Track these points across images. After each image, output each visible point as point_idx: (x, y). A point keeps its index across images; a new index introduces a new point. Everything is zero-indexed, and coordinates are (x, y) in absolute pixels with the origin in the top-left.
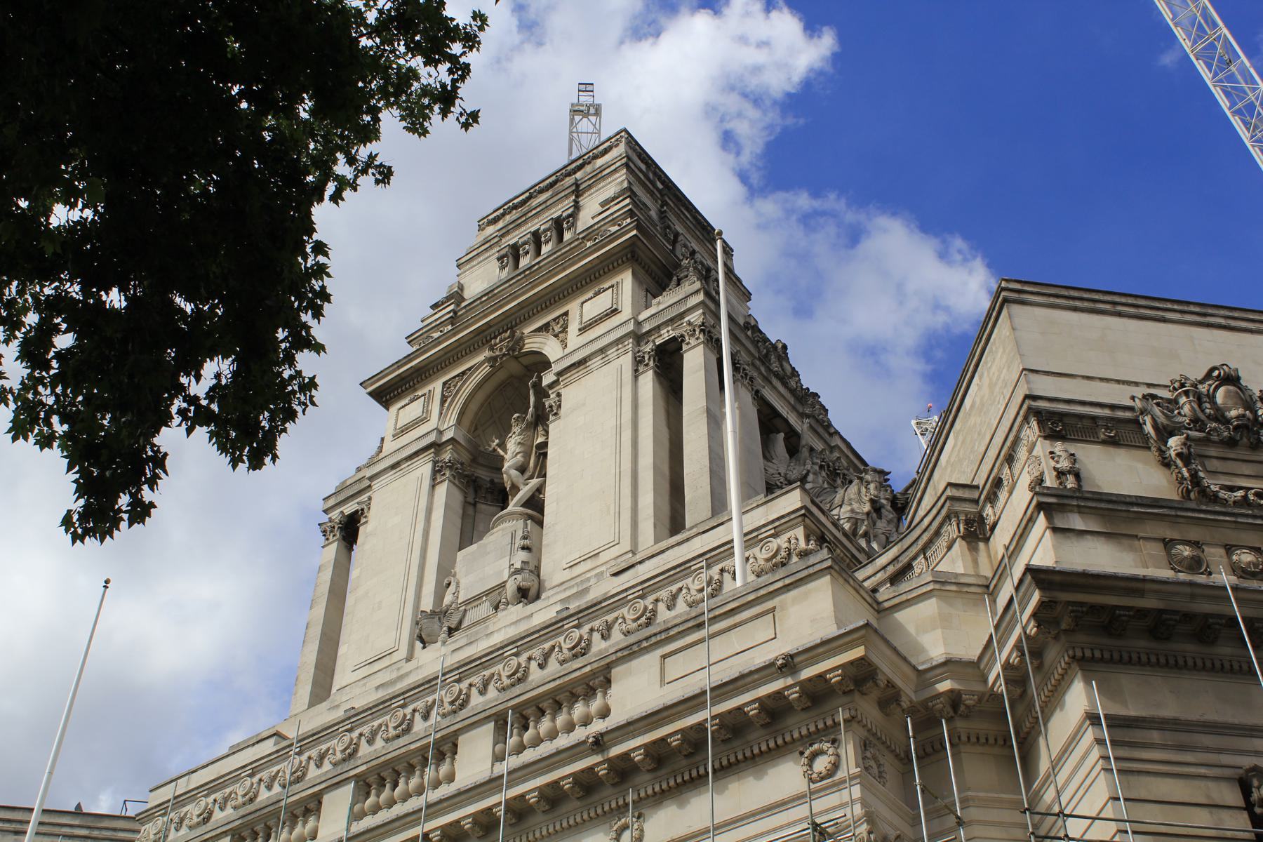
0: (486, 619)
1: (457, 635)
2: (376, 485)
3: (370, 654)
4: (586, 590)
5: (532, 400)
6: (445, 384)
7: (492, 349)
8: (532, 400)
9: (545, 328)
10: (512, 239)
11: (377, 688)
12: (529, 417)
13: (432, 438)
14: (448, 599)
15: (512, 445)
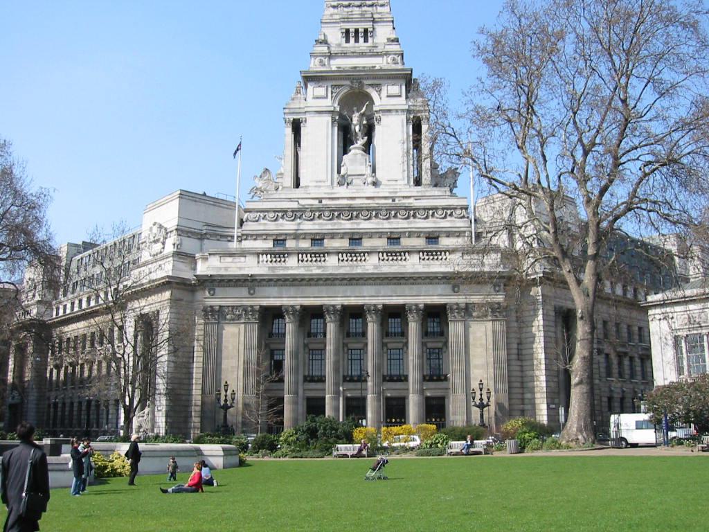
0: (360, 185)
1: (350, 187)
2: (307, 116)
3: (318, 179)
4: (396, 192)
5: (364, 109)
6: (332, 86)
7: (352, 82)
8: (364, 109)
9: (372, 85)
10: (347, 26)
11: (325, 193)
12: (362, 111)
13: (332, 109)
14: (343, 172)
15: (355, 120)
